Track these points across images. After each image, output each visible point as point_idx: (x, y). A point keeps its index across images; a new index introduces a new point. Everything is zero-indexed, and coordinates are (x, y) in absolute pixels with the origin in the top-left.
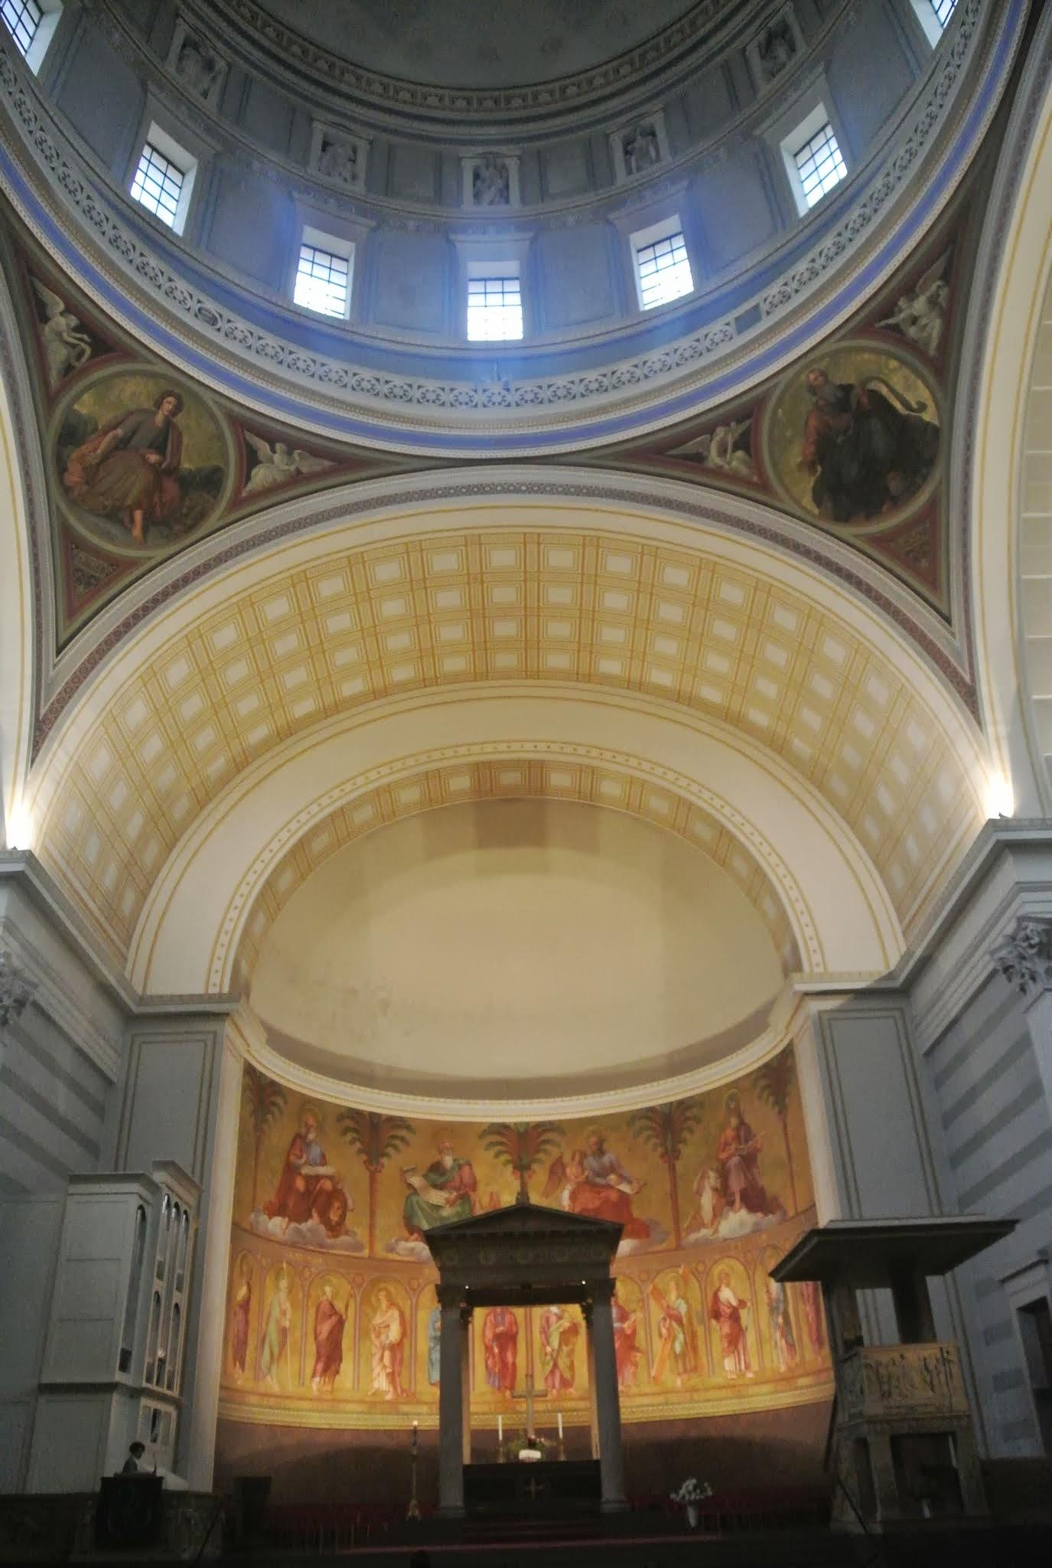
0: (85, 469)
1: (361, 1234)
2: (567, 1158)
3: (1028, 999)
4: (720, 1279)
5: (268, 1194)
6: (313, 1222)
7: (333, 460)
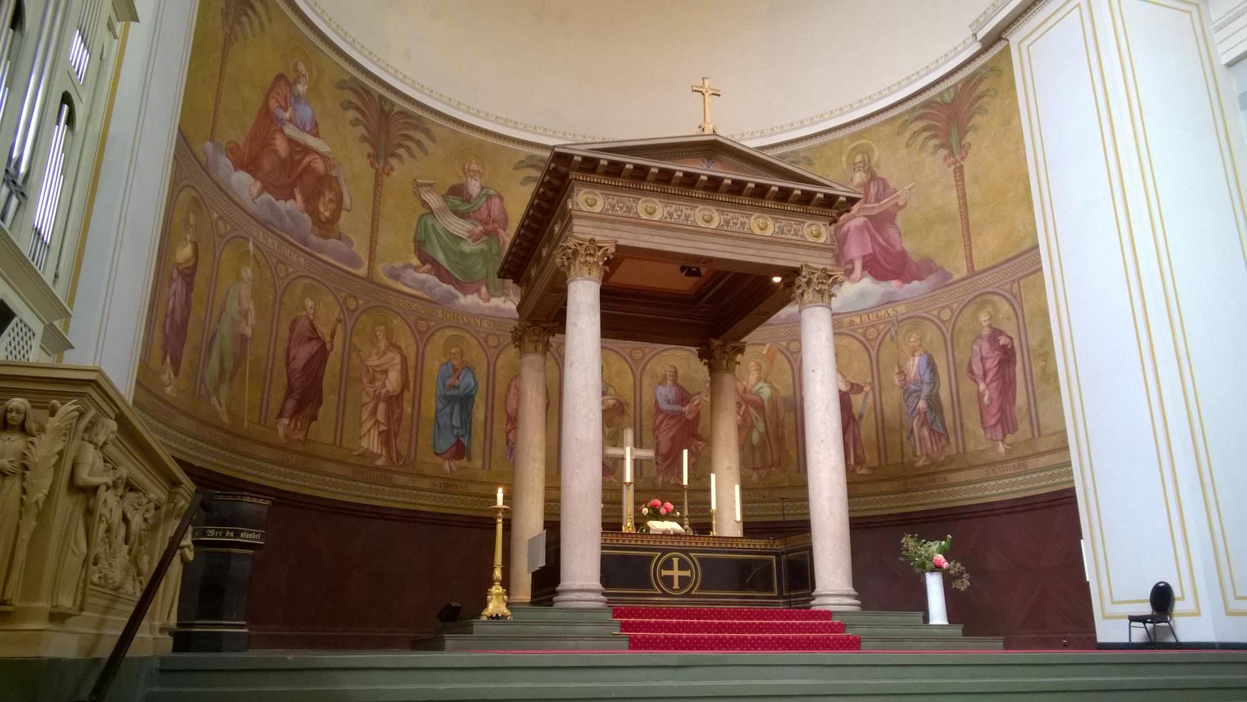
6: (294, 206)
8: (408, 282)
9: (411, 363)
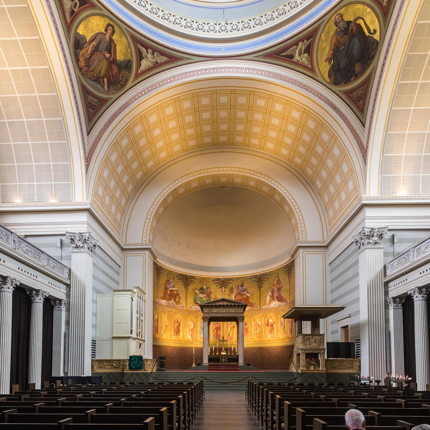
0: (85, 60)
1: (184, 304)
2: (234, 287)
3: (361, 250)
4: (269, 317)
5: (161, 294)
6: (172, 301)
7: (168, 57)
8: (193, 308)
9: (195, 323)
